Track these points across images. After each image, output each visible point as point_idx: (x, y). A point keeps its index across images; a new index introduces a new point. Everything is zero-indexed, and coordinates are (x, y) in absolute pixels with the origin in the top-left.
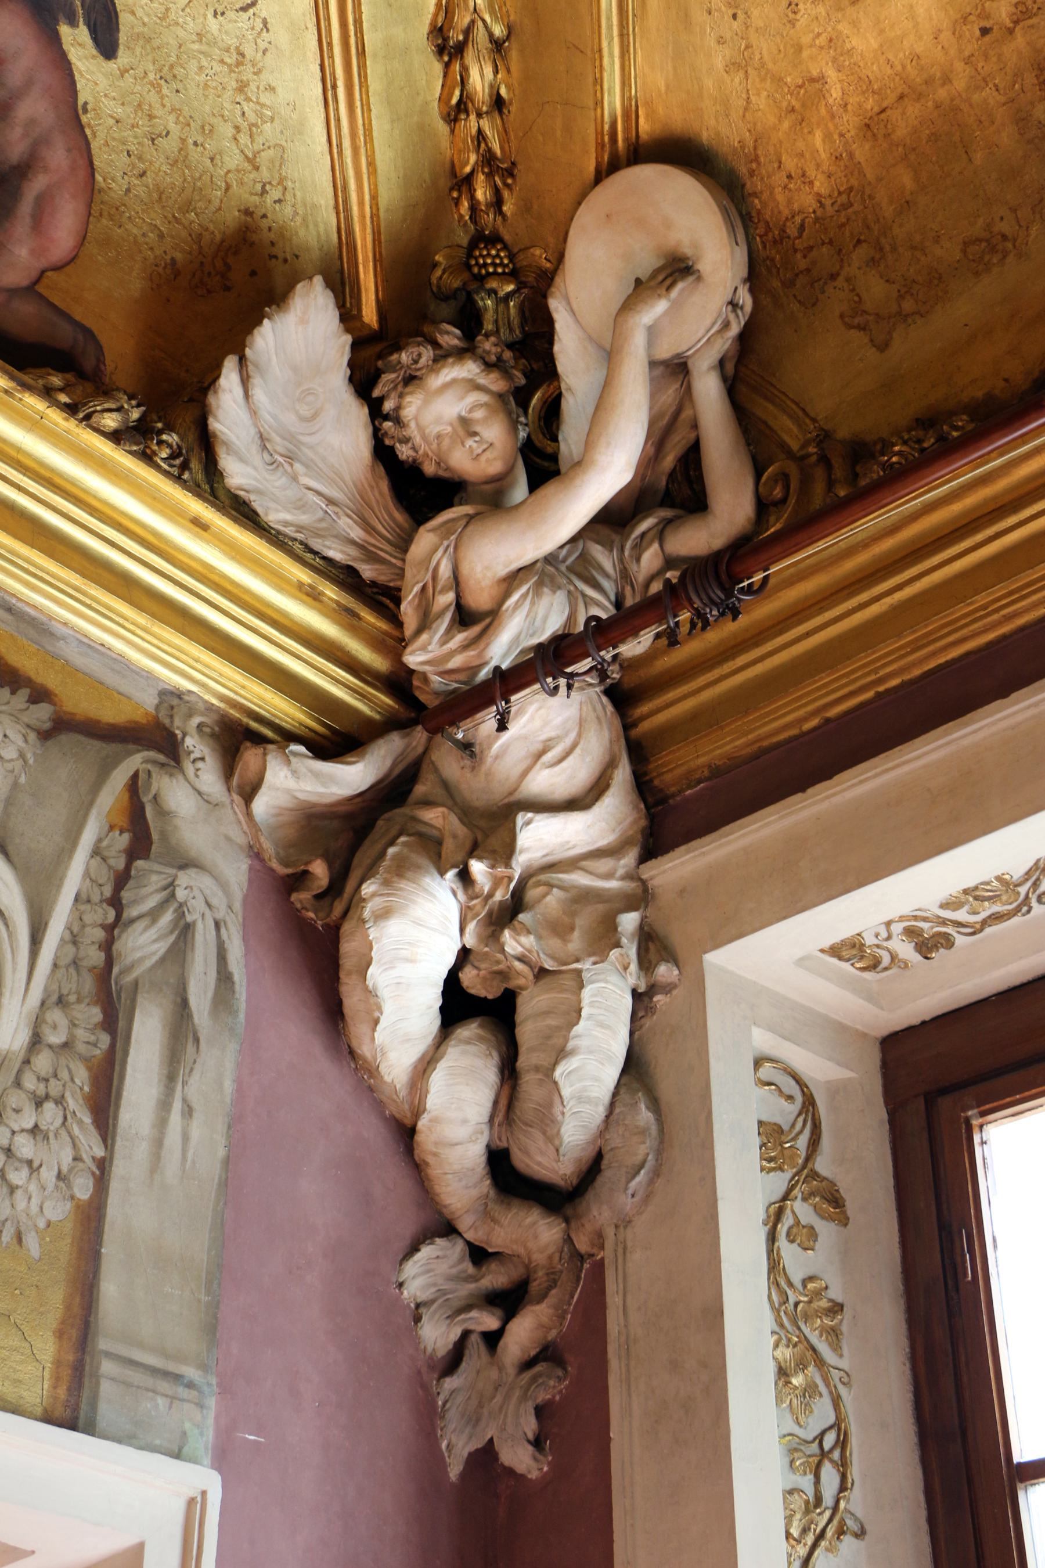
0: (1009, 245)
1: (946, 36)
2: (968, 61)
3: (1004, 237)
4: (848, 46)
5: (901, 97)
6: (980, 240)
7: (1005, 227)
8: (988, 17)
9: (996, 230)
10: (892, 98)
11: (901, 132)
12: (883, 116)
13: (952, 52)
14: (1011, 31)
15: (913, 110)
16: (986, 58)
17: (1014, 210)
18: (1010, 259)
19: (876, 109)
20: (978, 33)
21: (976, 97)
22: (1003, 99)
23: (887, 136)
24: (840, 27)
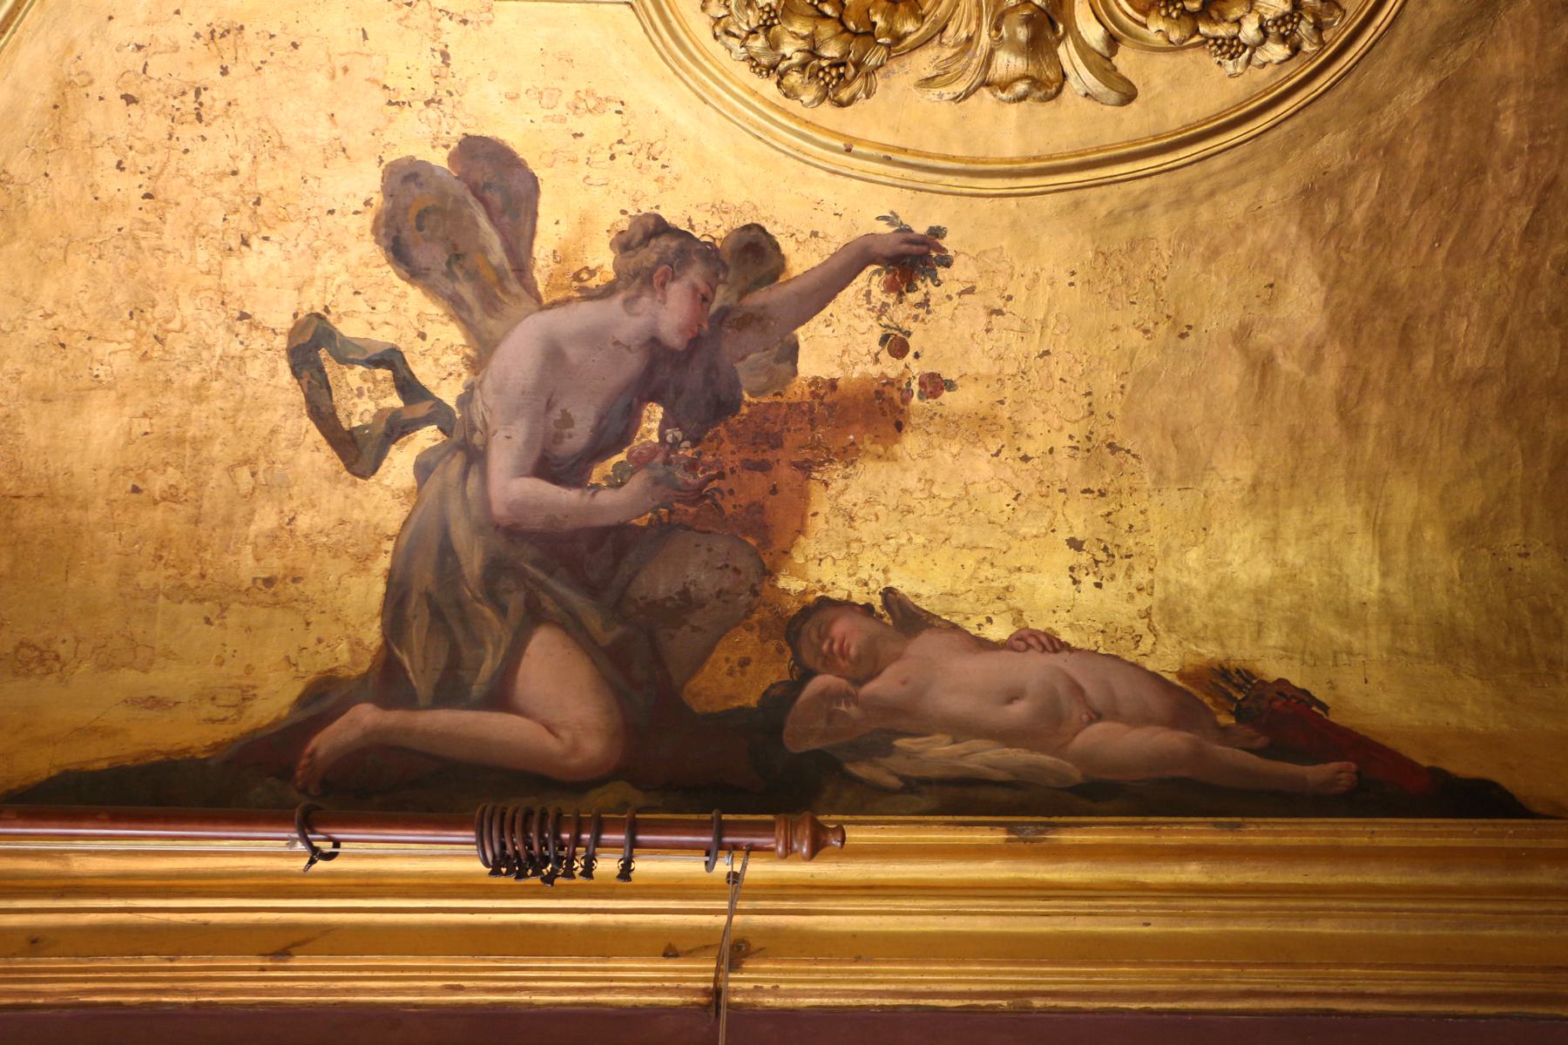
0: (57, 666)
1: (103, 474)
2: (110, 503)
3: (57, 658)
4: (20, 430)
5: (40, 496)
6: (36, 648)
7: (63, 650)
8: (144, 481)
9: (54, 647)
10: (32, 491)
11: (23, 522)
12: (15, 501)
13: (102, 488)
14: (156, 503)
15: (43, 513)
16: (126, 510)
17: (78, 641)
18: (52, 678)
19: (13, 492)
20: (129, 487)
21: (100, 534)
22: (120, 549)
23: (9, 518)
24: (22, 411)
